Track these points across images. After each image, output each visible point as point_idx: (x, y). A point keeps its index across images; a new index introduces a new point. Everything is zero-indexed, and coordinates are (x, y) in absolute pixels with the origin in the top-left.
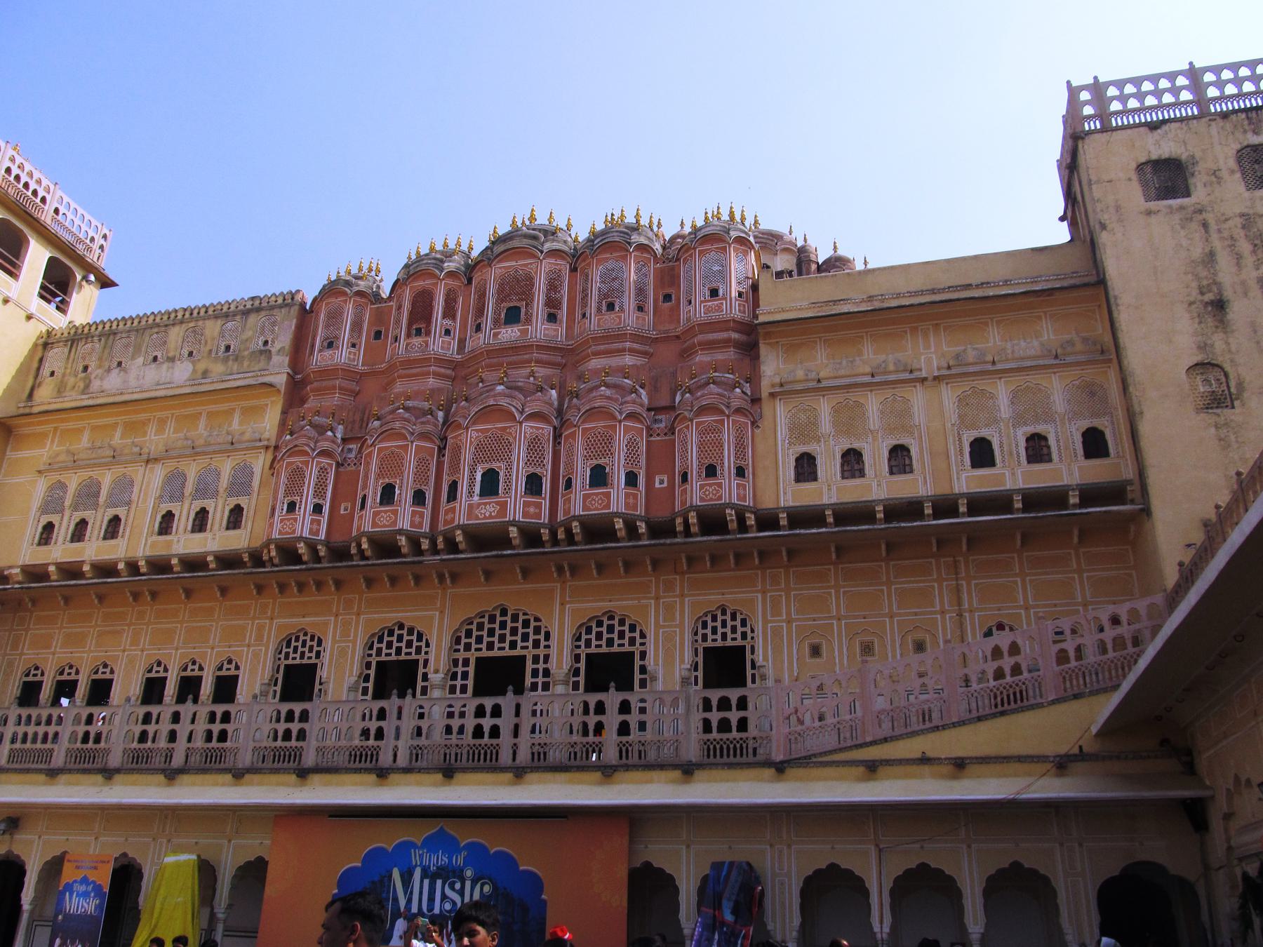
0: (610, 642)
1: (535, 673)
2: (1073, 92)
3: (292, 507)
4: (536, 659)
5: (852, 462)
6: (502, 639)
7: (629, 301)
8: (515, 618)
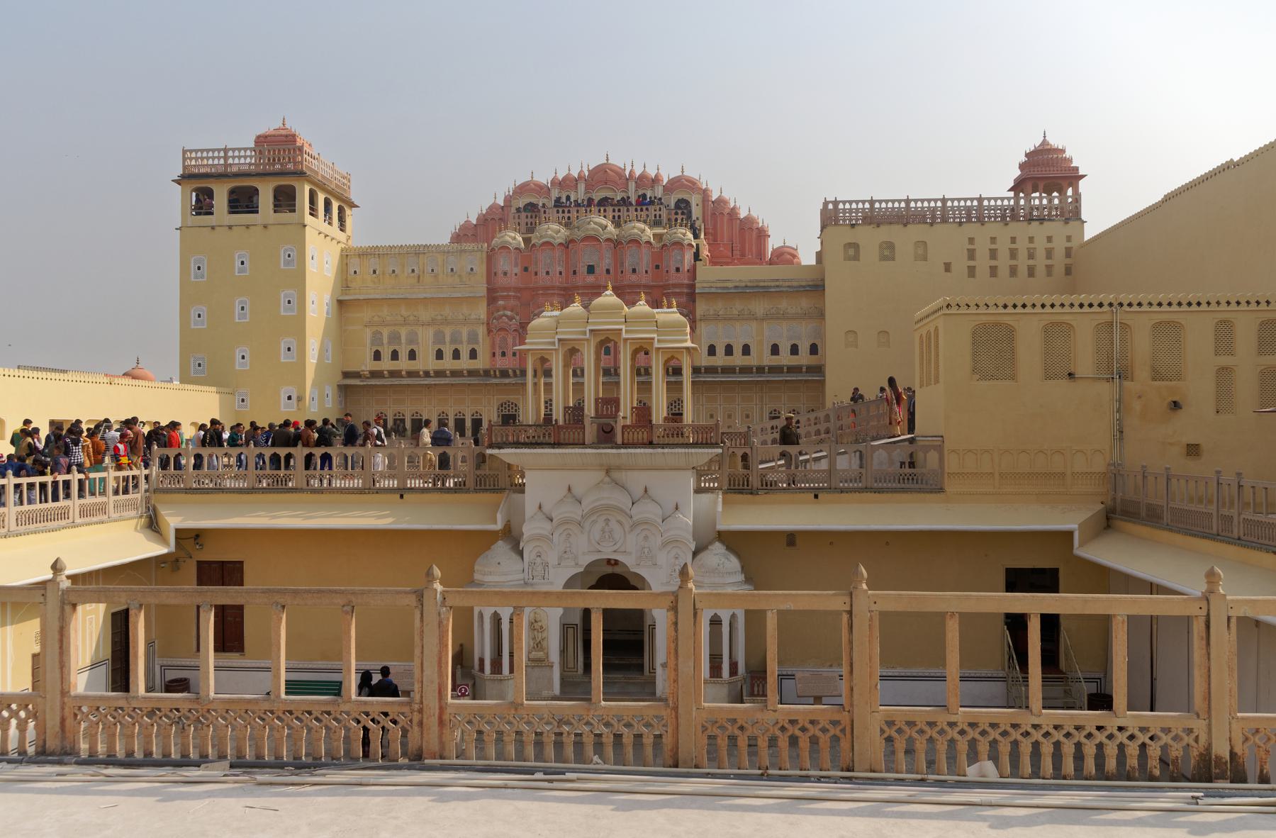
2: (826, 203)
3: (504, 354)
5: (729, 350)
7: (642, 269)
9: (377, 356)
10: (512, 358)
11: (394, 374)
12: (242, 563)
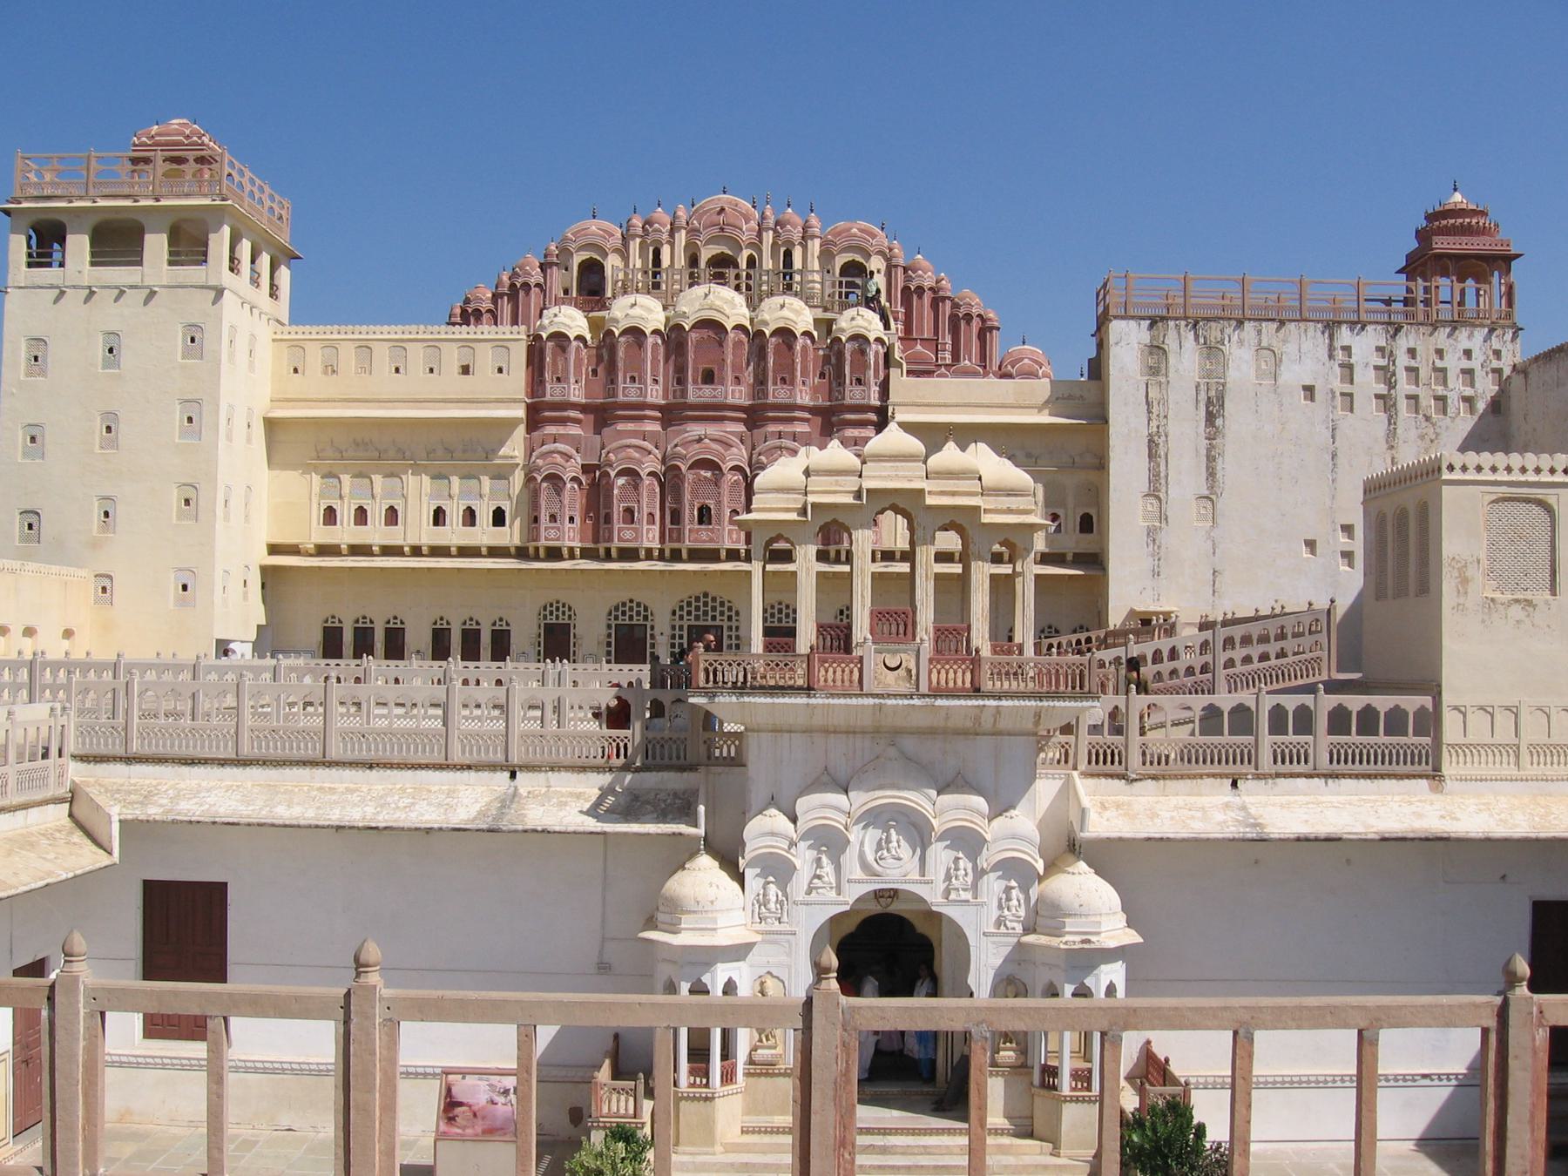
0: (780, 620)
1: (730, 637)
3: (553, 518)
4: (730, 628)
6: (705, 613)
8: (714, 599)
9: (330, 516)
10: (567, 525)
11: (357, 550)
12: (221, 888)
